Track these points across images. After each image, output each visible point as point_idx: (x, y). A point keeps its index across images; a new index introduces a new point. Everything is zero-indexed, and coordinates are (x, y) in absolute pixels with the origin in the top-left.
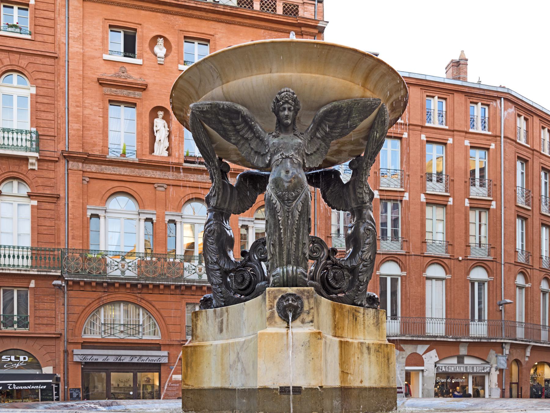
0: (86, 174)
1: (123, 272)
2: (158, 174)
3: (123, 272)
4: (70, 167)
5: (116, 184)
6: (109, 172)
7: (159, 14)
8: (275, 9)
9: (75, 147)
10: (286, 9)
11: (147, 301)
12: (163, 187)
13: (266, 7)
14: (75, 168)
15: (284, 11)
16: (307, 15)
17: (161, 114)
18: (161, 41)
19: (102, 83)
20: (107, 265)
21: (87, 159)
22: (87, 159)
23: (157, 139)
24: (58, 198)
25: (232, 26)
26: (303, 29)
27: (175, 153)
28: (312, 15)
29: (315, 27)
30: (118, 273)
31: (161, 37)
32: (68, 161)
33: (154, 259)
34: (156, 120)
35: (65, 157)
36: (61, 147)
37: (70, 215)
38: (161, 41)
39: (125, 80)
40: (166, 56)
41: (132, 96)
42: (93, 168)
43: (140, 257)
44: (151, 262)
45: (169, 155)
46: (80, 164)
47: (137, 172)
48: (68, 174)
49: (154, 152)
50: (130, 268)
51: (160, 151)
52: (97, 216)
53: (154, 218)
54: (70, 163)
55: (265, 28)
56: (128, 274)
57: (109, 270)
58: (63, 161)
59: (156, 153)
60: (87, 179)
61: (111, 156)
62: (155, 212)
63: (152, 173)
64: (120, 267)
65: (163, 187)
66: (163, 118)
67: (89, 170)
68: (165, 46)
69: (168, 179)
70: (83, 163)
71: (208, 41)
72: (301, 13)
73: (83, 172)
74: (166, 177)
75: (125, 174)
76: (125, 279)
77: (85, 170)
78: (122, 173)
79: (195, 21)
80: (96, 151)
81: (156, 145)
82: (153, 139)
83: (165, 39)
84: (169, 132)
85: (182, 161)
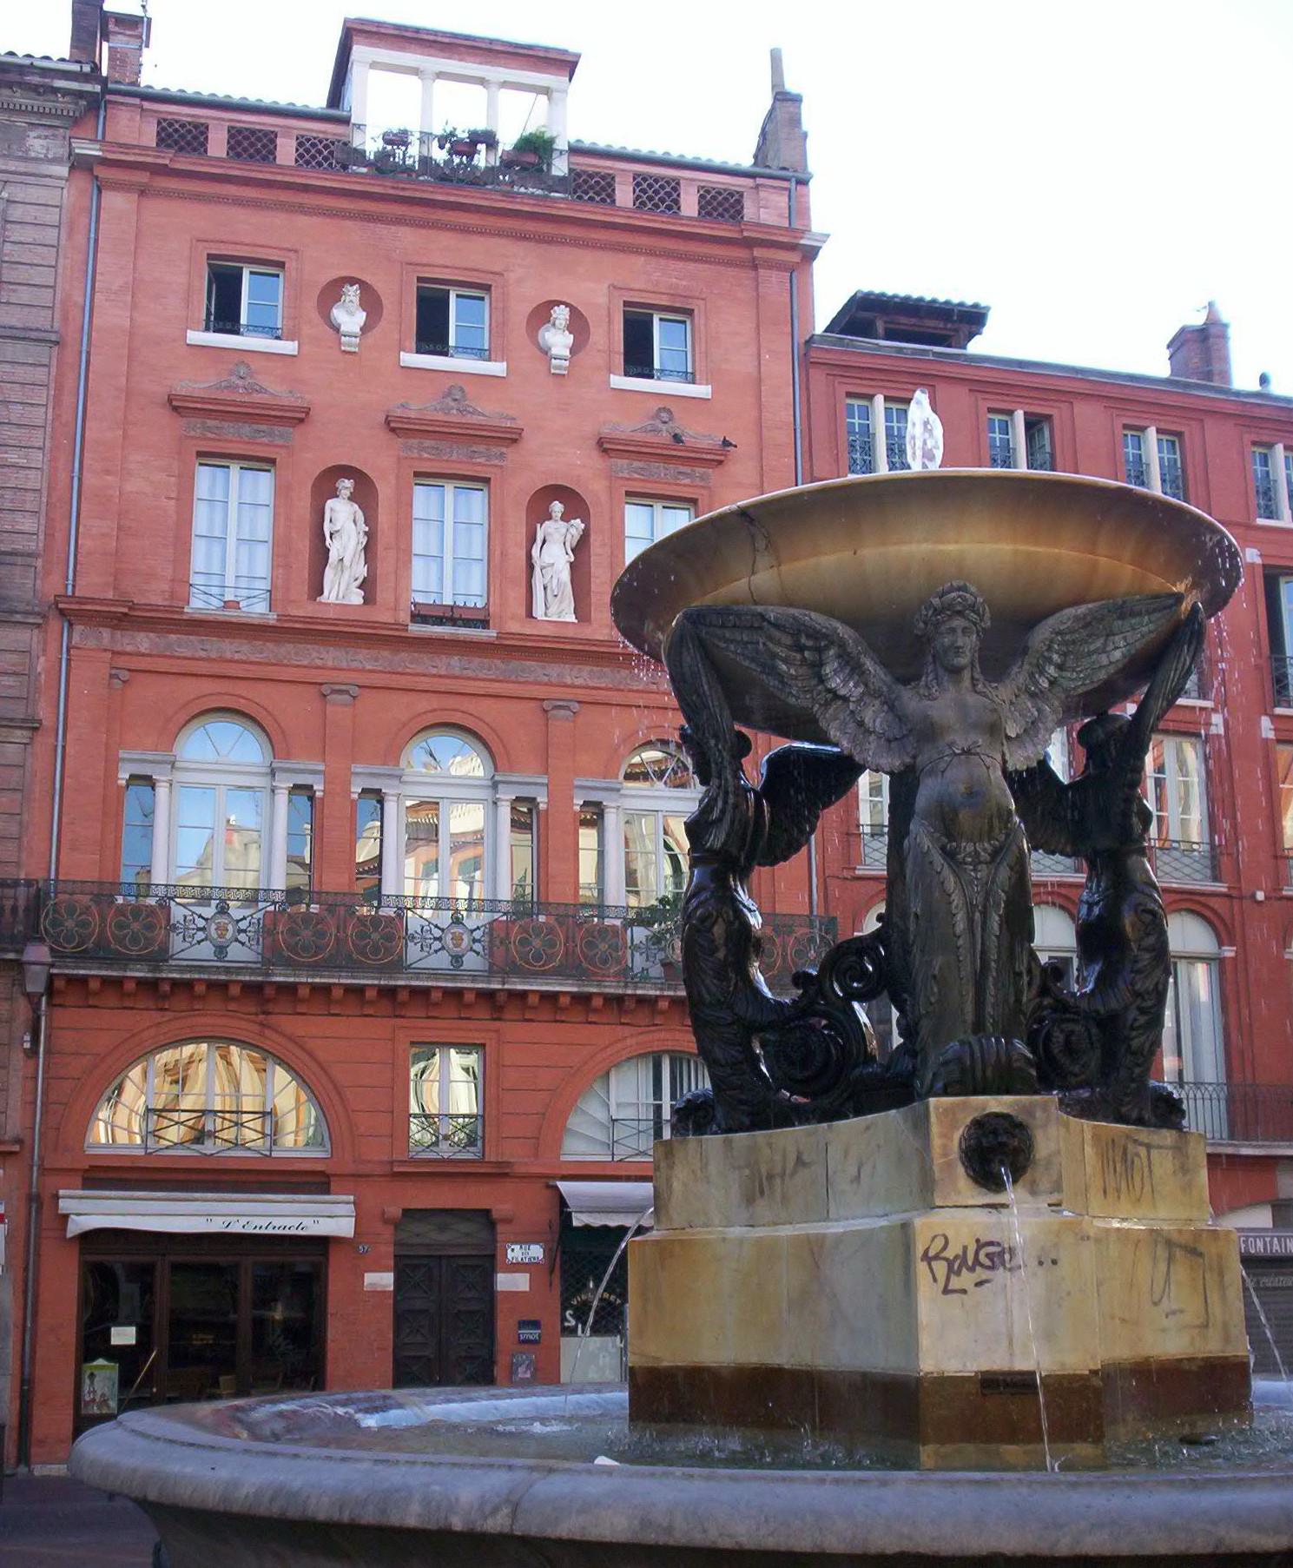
0: (122, 662)
1: (221, 950)
2: (331, 656)
3: (221, 950)
4: (76, 639)
5: (208, 686)
6: (189, 654)
7: (348, 223)
8: (676, 202)
9: (93, 585)
10: (709, 203)
11: (290, 1038)
12: (347, 692)
13: (650, 199)
14: (92, 643)
15: (701, 208)
16: (767, 217)
17: (346, 485)
18: (352, 293)
19: (178, 406)
20: (174, 928)
21: (126, 618)
22: (126, 618)
23: (333, 556)
24: (35, 729)
25: (554, 250)
26: (757, 252)
27: (384, 594)
28: (780, 216)
29: (793, 247)
30: (205, 951)
31: (352, 281)
32: (71, 625)
33: (314, 908)
34: (330, 503)
35: (62, 613)
36: (52, 586)
37: (67, 781)
38: (352, 293)
39: (246, 399)
40: (365, 329)
41: (265, 440)
42: (143, 641)
43: (274, 903)
44: (307, 917)
45: (369, 600)
46: (106, 633)
47: (270, 650)
48: (69, 661)
49: (322, 593)
50: (242, 937)
51: (342, 588)
52: (148, 781)
53: (319, 788)
54: (78, 628)
55: (651, 253)
56: (237, 953)
57: (177, 942)
58: (55, 624)
59: (331, 594)
60: (125, 675)
61: (199, 604)
62: (322, 767)
63: (315, 654)
64: (214, 934)
65: (347, 692)
66: (352, 498)
67: (129, 649)
68: (364, 304)
69: (363, 670)
70: (114, 628)
71: (487, 288)
72: (749, 212)
73: (114, 653)
74: (355, 665)
75: (237, 657)
76: (227, 970)
77: (118, 648)
78: (228, 655)
79: (445, 239)
80: (154, 595)
81: (329, 573)
82: (321, 555)
83: (365, 288)
84: (371, 536)
85: (404, 617)
